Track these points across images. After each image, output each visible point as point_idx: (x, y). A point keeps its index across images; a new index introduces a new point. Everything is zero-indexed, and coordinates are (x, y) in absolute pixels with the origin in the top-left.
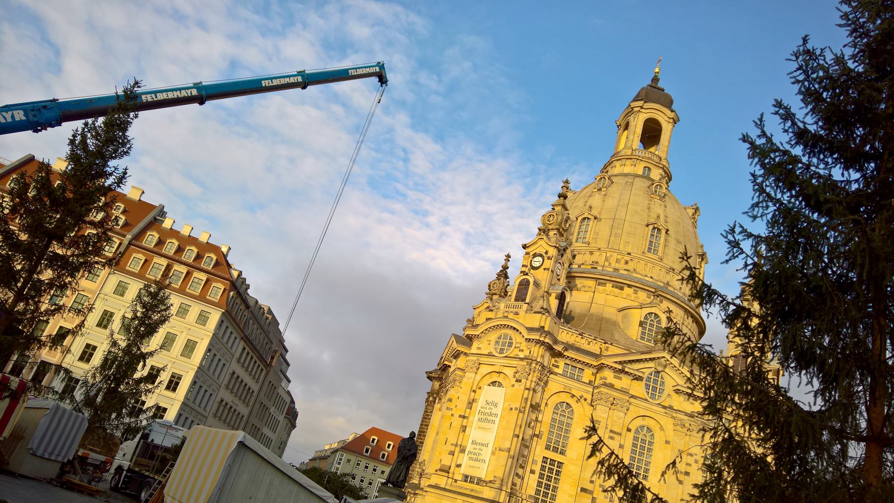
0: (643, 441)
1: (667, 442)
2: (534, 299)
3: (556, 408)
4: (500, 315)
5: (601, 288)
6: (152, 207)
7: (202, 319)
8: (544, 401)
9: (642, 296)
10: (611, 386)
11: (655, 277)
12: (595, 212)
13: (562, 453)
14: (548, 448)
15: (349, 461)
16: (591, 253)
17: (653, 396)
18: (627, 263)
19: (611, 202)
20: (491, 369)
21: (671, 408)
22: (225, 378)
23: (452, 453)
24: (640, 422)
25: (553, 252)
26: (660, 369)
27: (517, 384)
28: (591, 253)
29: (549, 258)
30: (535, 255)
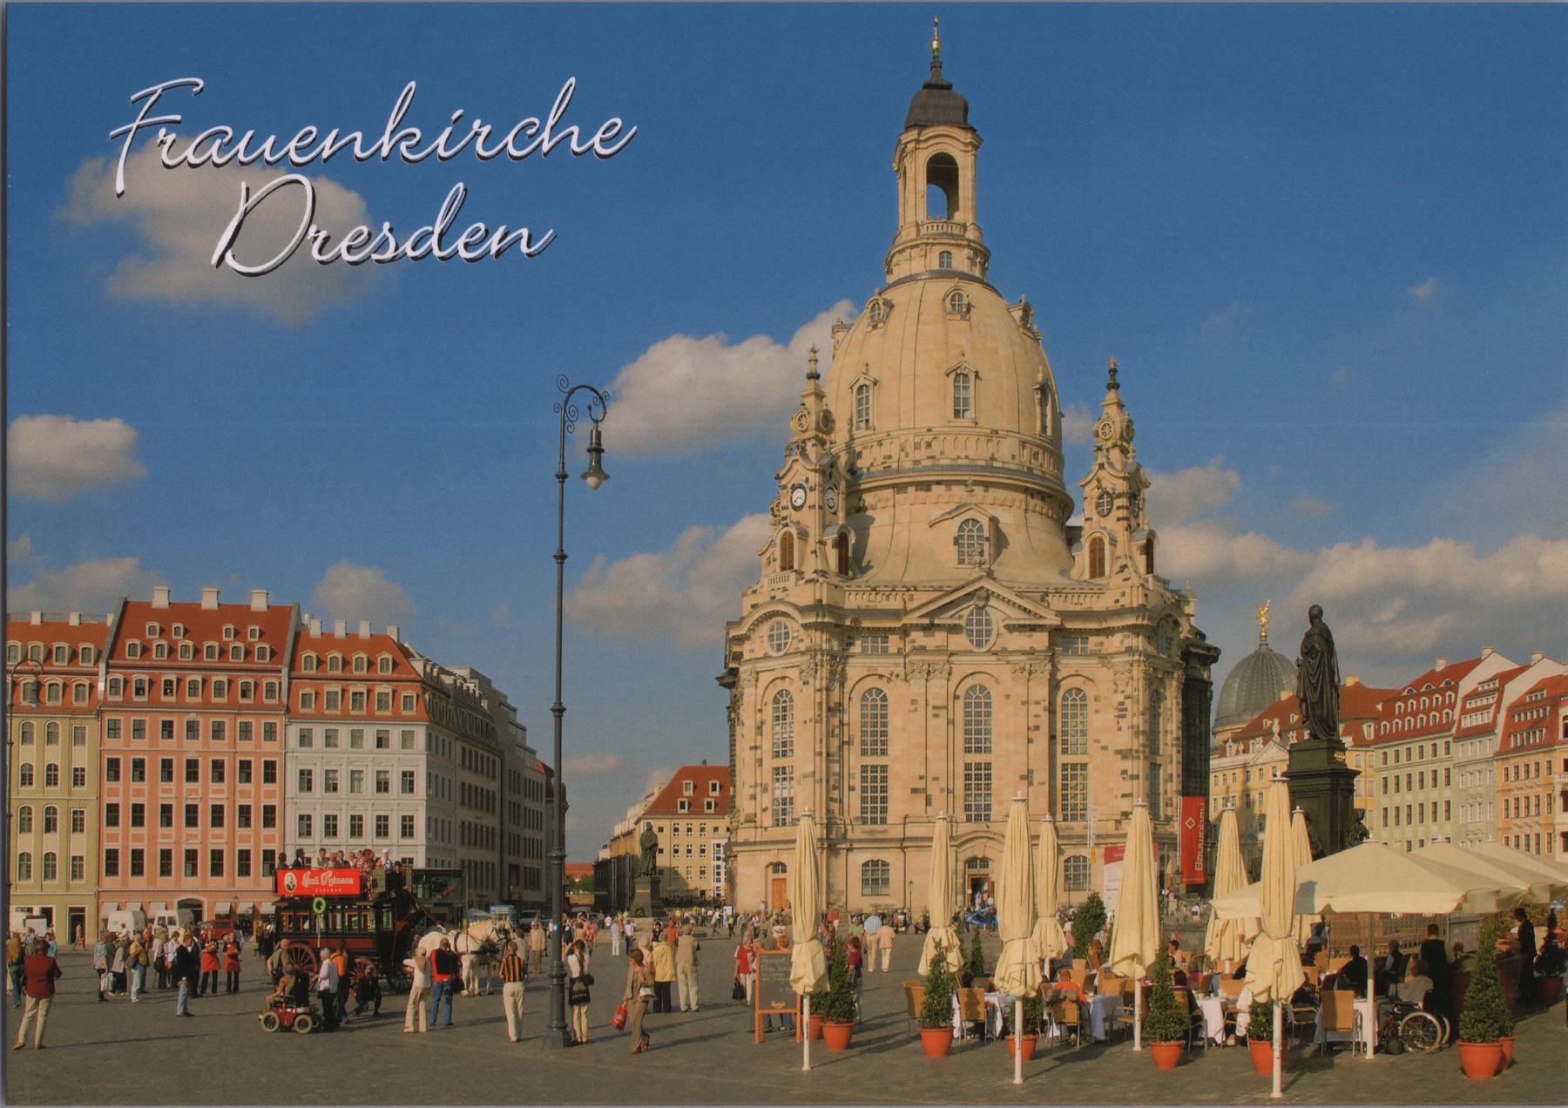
0: (978, 705)
3: (864, 698)
5: (900, 497)
8: (846, 697)
9: (958, 491)
12: (873, 374)
13: (884, 752)
14: (864, 753)
17: (979, 644)
23: (754, 797)
25: (815, 478)
26: (981, 604)
27: (805, 688)
28: (880, 443)
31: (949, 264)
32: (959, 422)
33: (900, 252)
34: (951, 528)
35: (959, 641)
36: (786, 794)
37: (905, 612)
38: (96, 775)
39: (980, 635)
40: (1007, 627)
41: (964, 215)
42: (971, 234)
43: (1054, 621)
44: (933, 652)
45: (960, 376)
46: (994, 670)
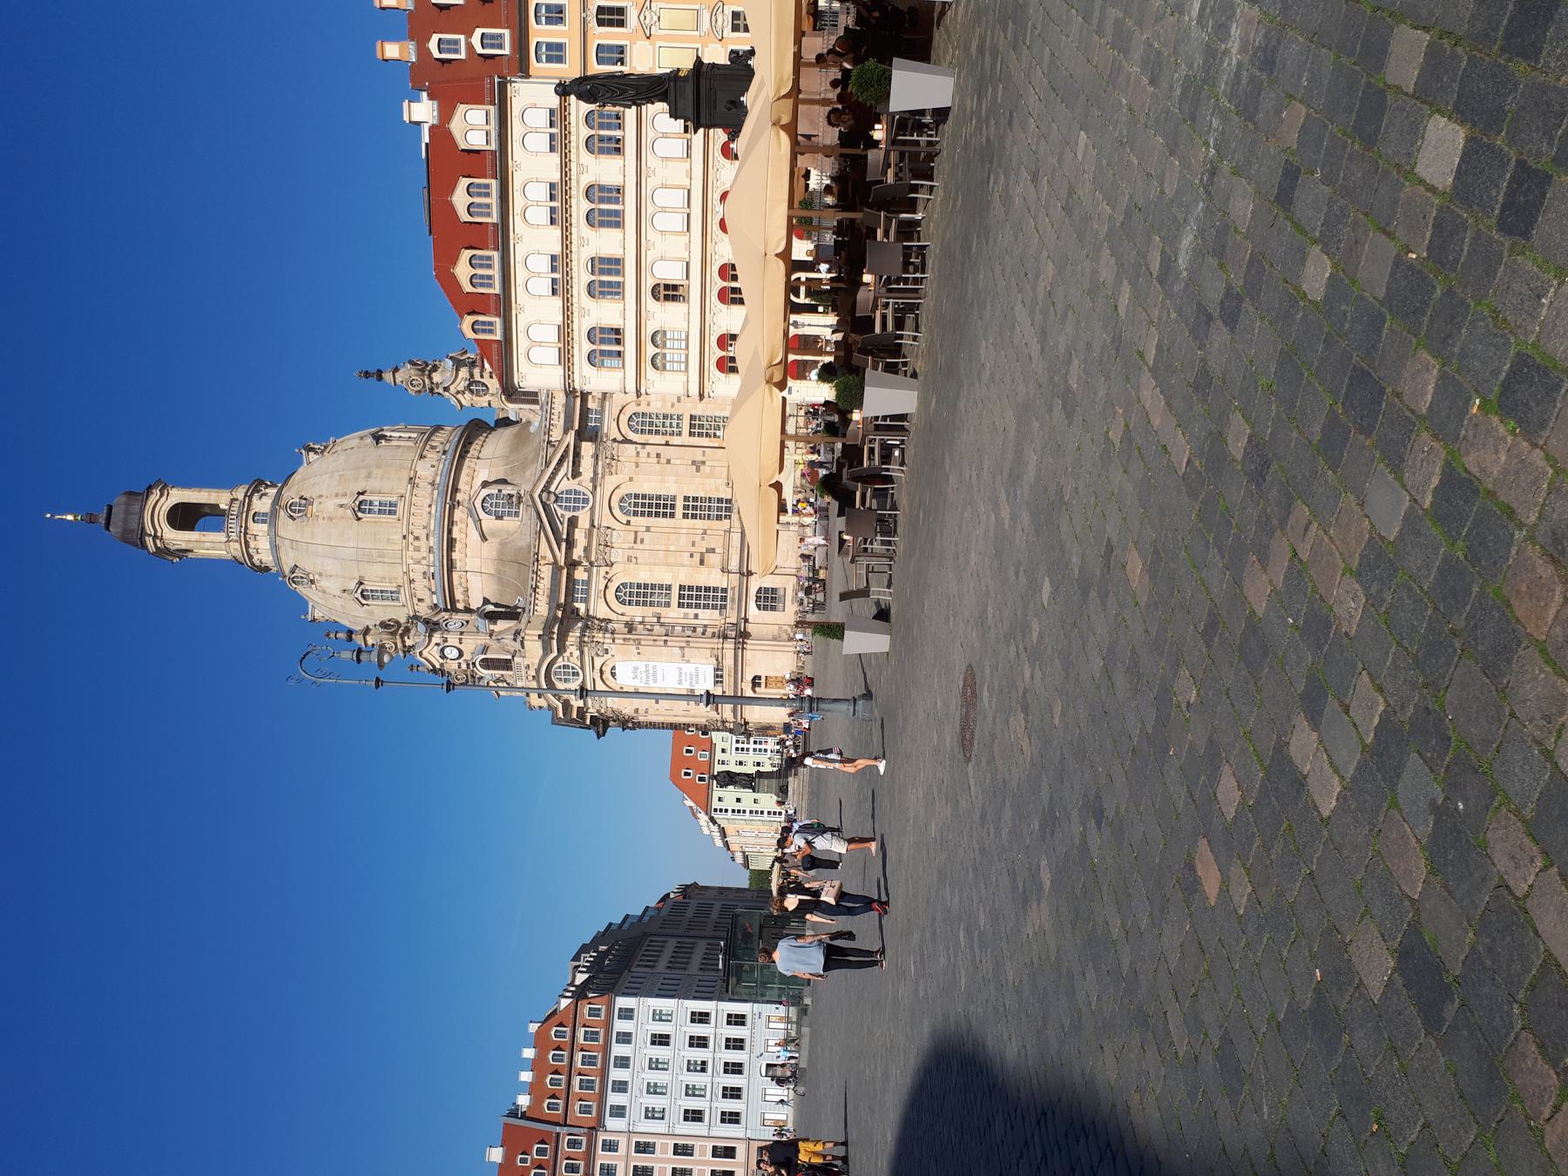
0: (636, 505)
1: (631, 479)
5: (458, 564)
7: (627, 1014)
9: (459, 514)
10: (587, 549)
11: (428, 501)
12: (352, 585)
13: (669, 587)
14: (668, 605)
16: (411, 581)
17: (586, 501)
18: (417, 538)
19: (330, 566)
21: (594, 480)
24: (616, 511)
26: (553, 498)
28: (411, 581)
29: (445, 640)
30: (443, 656)
31: (265, 514)
32: (400, 509)
33: (251, 557)
34: (489, 522)
35: (584, 522)
37: (555, 563)
39: (578, 500)
40: (574, 477)
41: (221, 498)
42: (240, 493)
43: (570, 438)
45: (361, 507)
46: (608, 489)
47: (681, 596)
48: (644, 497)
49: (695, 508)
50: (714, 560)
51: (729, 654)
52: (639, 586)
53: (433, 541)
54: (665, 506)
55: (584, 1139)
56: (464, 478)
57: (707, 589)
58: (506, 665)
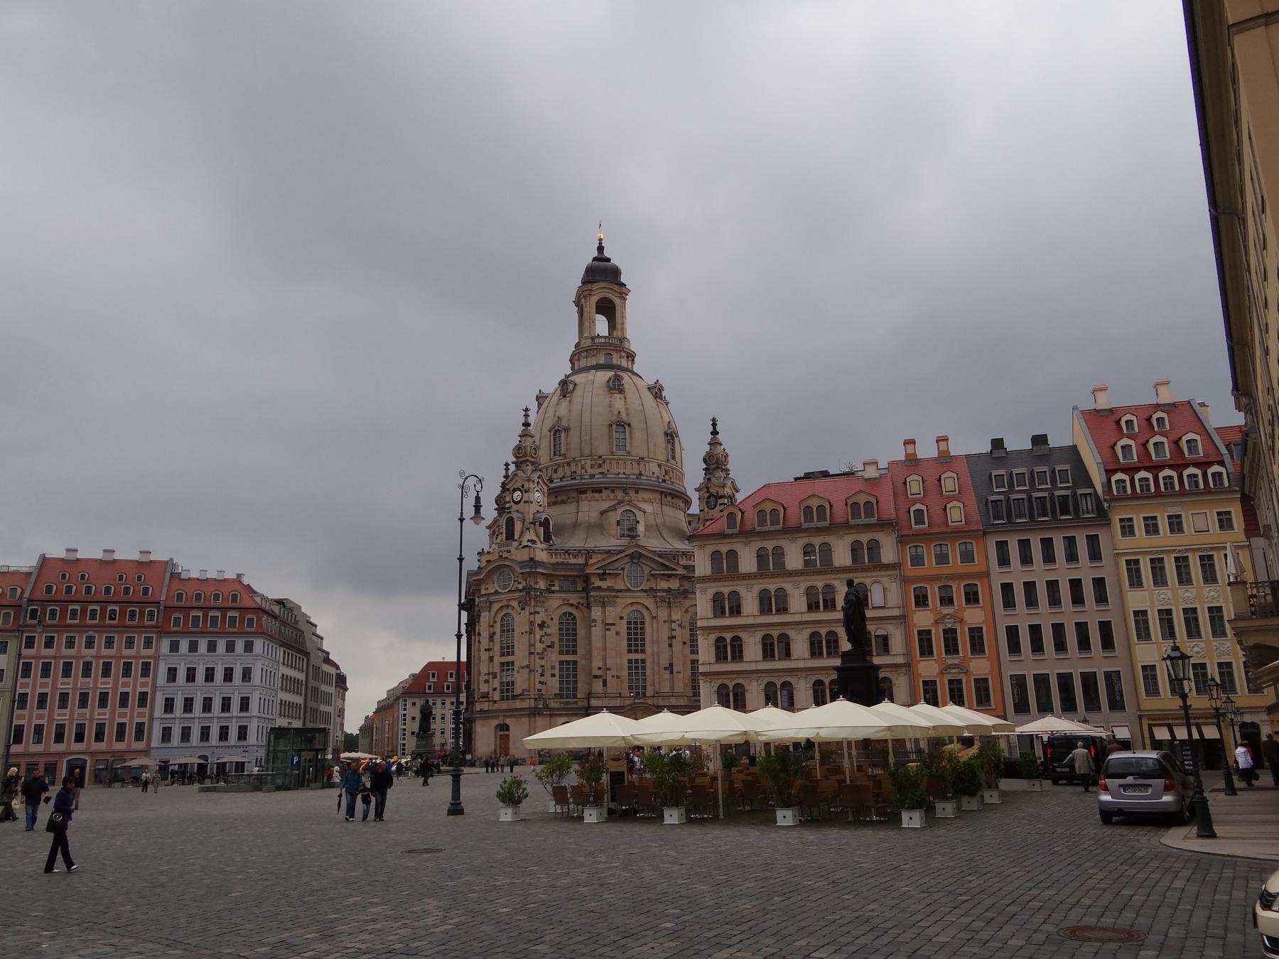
1: (654, 618)
2: (522, 533)
4: (496, 557)
6: (166, 562)
7: (249, 647)
9: (620, 494)
10: (599, 588)
12: (565, 424)
13: (575, 652)
14: (561, 653)
15: (414, 704)
16: (569, 464)
20: (499, 605)
22: (278, 683)
23: (487, 681)
28: (569, 464)
30: (514, 490)
36: (509, 679)
38: (11, 674)
43: (681, 571)
44: (604, 590)
47: (568, 662)
48: (642, 628)
49: (637, 668)
50: (598, 686)
51: (525, 704)
52: (575, 629)
53: (598, 478)
54: (636, 645)
55: (153, 623)
56: (647, 495)
57: (575, 682)
58: (510, 536)
